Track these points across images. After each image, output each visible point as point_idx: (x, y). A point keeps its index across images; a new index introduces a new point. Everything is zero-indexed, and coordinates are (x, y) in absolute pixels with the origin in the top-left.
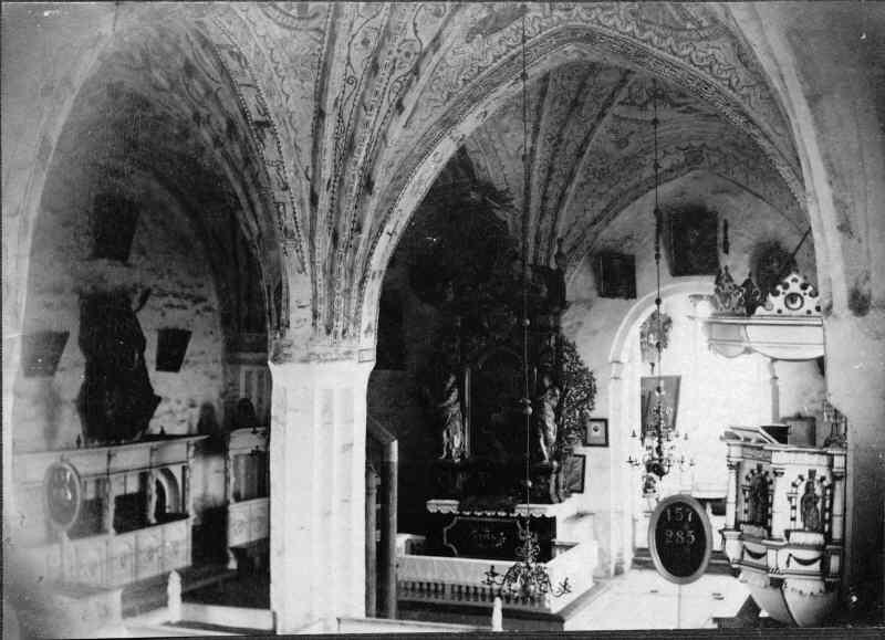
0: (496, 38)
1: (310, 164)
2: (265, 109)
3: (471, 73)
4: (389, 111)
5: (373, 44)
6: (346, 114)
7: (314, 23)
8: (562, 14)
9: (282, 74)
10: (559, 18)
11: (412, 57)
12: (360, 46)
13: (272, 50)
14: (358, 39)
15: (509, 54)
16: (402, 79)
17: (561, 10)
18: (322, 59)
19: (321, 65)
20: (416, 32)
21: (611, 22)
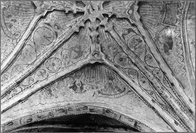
0: (174, 46)
1: (167, 125)
2: (132, 119)
3: (182, 58)
4: (172, 89)
5: (147, 81)
6: (161, 102)
7: (126, 91)
8: (178, 22)
9: (131, 108)
10: (179, 24)
11: (159, 72)
12: (144, 84)
13: (121, 105)
14: (141, 83)
15: (183, 44)
16: (165, 79)
17: (176, 22)
18: (139, 97)
19: (141, 98)
20: (152, 67)
21: (182, 4)
